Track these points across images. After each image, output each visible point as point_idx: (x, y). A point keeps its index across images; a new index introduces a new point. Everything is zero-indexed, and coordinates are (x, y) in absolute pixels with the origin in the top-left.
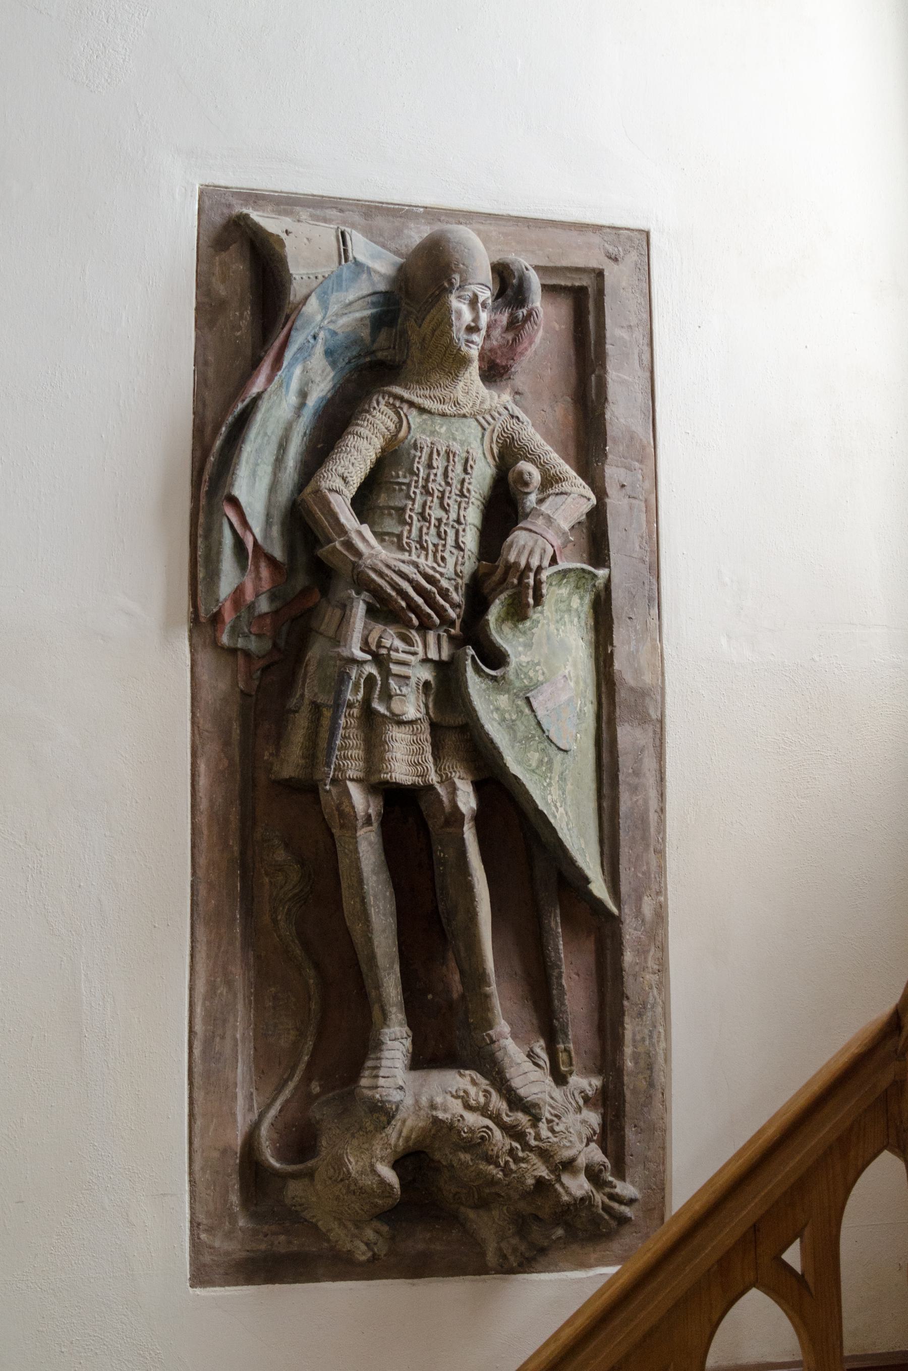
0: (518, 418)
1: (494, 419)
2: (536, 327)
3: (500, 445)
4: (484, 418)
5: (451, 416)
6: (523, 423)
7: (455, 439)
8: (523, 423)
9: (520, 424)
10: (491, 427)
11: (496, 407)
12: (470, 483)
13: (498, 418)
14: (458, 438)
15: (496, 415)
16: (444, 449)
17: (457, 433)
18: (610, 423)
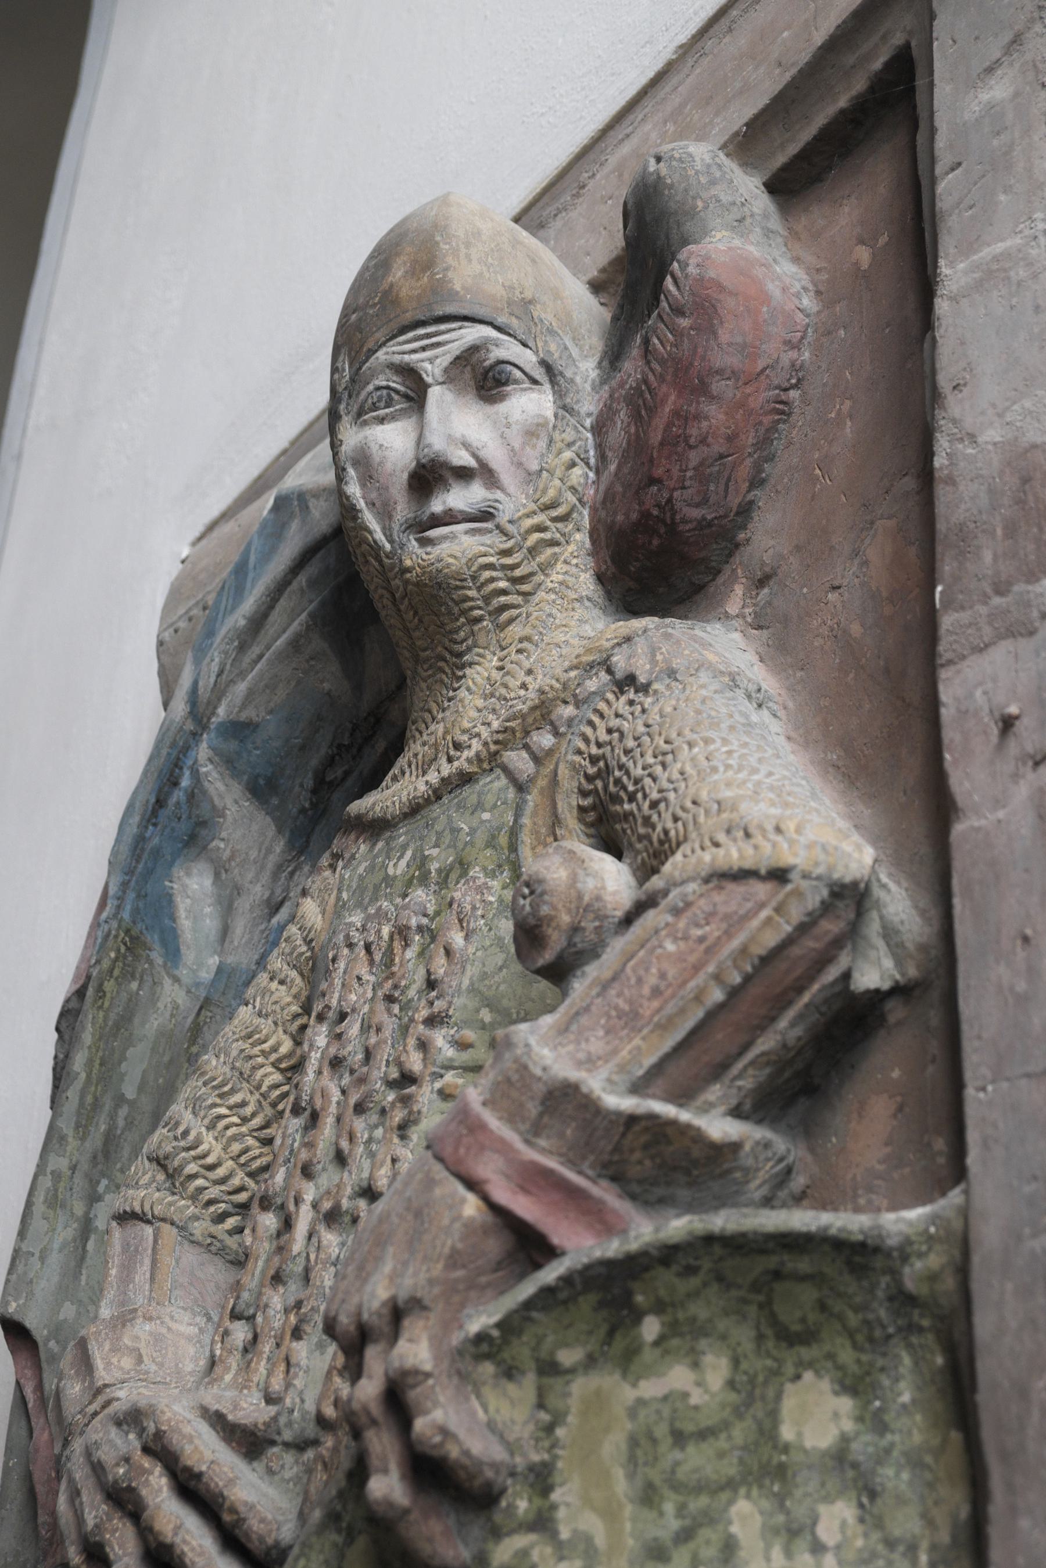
0: (630, 679)
1: (556, 733)
2: (684, 323)
3: (591, 816)
4: (526, 747)
5: (428, 802)
6: (645, 689)
7: (424, 880)
9: (640, 697)
11: (565, 686)
12: (431, 1021)
13: (570, 723)
14: (434, 866)
16: (386, 931)
17: (435, 852)
18: (951, 481)
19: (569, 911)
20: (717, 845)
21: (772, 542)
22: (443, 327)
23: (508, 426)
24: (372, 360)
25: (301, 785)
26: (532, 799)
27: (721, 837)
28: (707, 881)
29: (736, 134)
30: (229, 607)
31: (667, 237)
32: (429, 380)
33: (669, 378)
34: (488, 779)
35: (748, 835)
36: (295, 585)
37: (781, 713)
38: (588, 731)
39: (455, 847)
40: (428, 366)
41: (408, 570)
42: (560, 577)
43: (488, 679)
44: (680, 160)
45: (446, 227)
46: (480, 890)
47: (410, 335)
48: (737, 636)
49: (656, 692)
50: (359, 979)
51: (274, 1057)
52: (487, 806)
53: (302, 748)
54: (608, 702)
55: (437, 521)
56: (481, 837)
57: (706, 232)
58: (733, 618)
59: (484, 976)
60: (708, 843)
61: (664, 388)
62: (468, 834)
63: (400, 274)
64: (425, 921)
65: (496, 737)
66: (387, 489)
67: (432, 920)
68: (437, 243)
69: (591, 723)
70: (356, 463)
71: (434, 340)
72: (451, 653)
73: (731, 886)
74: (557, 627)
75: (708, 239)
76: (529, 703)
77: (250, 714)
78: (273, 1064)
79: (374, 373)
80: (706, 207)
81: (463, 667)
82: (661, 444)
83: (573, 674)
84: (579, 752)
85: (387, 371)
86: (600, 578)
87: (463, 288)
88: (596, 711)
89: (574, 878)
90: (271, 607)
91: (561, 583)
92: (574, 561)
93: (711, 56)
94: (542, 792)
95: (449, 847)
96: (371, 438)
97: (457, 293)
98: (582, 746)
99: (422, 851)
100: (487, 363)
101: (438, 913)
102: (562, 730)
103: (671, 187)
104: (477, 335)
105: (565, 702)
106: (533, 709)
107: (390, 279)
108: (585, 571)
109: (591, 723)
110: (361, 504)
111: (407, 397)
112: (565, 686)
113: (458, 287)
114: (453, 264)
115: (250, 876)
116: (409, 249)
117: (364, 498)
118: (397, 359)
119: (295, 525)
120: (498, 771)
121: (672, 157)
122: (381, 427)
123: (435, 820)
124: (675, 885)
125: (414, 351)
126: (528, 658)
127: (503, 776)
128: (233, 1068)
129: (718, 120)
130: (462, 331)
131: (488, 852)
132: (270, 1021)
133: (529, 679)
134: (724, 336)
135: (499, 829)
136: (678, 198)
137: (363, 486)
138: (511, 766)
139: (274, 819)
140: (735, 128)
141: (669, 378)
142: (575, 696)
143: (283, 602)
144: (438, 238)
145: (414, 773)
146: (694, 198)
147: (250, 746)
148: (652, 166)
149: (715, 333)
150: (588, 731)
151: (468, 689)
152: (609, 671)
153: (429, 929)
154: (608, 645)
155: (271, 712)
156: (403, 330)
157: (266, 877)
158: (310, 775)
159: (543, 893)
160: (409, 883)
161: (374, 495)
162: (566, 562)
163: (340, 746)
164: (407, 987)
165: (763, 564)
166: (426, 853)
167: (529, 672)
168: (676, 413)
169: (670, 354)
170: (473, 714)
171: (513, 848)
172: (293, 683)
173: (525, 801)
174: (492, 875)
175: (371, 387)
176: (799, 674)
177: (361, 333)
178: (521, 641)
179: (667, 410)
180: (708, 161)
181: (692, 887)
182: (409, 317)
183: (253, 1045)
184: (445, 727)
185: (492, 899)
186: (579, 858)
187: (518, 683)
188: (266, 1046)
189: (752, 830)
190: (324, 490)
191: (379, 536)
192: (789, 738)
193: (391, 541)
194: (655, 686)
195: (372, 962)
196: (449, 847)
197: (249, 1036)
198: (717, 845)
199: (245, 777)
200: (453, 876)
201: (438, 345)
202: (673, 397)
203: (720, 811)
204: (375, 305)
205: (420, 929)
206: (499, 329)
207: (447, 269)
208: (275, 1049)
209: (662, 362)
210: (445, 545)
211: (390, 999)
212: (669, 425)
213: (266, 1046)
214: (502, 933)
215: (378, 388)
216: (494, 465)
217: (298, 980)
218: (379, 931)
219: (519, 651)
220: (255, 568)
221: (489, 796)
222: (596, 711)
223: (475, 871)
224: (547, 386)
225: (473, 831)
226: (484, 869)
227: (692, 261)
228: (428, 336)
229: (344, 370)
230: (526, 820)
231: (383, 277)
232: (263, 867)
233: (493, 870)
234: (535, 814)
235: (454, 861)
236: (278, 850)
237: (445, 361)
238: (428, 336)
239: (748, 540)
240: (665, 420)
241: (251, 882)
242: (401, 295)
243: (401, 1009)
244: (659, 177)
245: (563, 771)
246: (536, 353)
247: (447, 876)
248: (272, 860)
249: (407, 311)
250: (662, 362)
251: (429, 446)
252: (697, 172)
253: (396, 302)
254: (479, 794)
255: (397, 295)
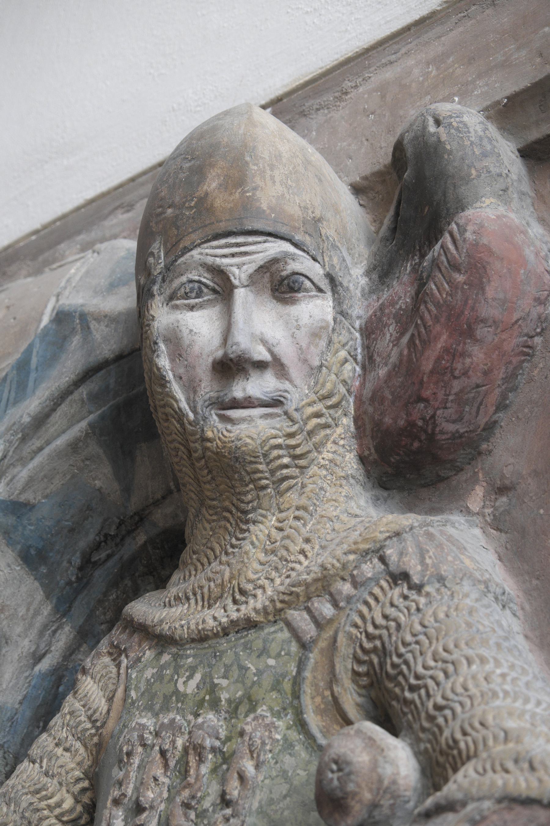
0: (405, 576)
1: (335, 604)
2: (460, 278)
3: (365, 681)
4: (308, 610)
5: (216, 635)
6: (419, 588)
7: (215, 704)
8: (419, 588)
9: (413, 595)
10: (328, 634)
11: (344, 566)
13: (349, 599)
14: (224, 696)
15: (346, 588)
16: (180, 742)
17: (224, 682)
19: (371, 790)
20: (507, 771)
21: (512, 460)
22: (251, 239)
23: (298, 328)
24: (187, 256)
25: (70, 562)
26: (313, 657)
27: (510, 765)
28: (500, 801)
29: (498, 103)
30: (12, 400)
31: (444, 194)
32: (236, 282)
33: (443, 320)
34: (272, 629)
35: (532, 768)
36: (76, 395)
37: (520, 613)
38: (365, 610)
39: (243, 683)
40: (235, 270)
41: (209, 440)
42: (330, 456)
43: (269, 536)
44: (458, 129)
45: (254, 148)
46: (270, 727)
47: (223, 241)
48: (477, 531)
49: (428, 594)
50: (156, 779)
51: (57, 811)
52: (273, 653)
53: (72, 530)
54: (382, 588)
55: (236, 404)
56: (267, 681)
57: (477, 198)
58: (474, 514)
59: (271, 802)
60: (498, 768)
61: (438, 328)
62: (255, 674)
63: (214, 185)
64: (217, 743)
65: (282, 597)
66: (194, 367)
67: (224, 743)
68: (247, 163)
69: (366, 603)
70: (167, 340)
71: (243, 249)
72: (238, 509)
73: (519, 809)
74: (328, 501)
75: (478, 204)
76: (312, 575)
77: (28, 496)
78: (57, 817)
79: (187, 268)
80: (479, 176)
81: (247, 522)
82: (432, 372)
83: (352, 557)
84: (356, 626)
85: (200, 268)
86: (362, 459)
87: (270, 208)
88: (371, 594)
89: (375, 765)
90: (53, 410)
91: (331, 461)
92: (342, 442)
93: (473, 21)
94: (322, 651)
95: (237, 681)
96: (182, 323)
97: (264, 211)
98: (359, 621)
99: (212, 678)
100: (284, 273)
101: (229, 739)
102: (342, 604)
103: (450, 153)
104: (278, 250)
105: (343, 579)
106: (316, 580)
107: (205, 187)
108: (350, 451)
109: (366, 603)
110: (170, 376)
111: (214, 291)
112: (344, 566)
113: (264, 206)
114: (261, 184)
115: (18, 629)
116: (221, 163)
117: (172, 370)
118: (210, 260)
119: (76, 340)
120: (282, 624)
121: (450, 124)
122: (190, 314)
123: (223, 652)
124: (473, 799)
125: (225, 256)
126: (304, 525)
127: (285, 629)
128: (23, 817)
129: (480, 83)
130: (267, 245)
131: (274, 695)
132: (55, 781)
133: (307, 547)
134: (490, 292)
135: (284, 676)
136: (456, 164)
137: (172, 361)
138: (295, 624)
139: (42, 585)
140: (497, 98)
141: (443, 320)
142: (352, 576)
143: (64, 407)
144: (248, 159)
145: (200, 603)
146: (469, 167)
147: (25, 522)
148: (432, 128)
149: (483, 289)
150: (365, 610)
151: (252, 543)
152: (383, 559)
153: (221, 751)
154: (381, 537)
155: (46, 497)
156: (217, 237)
157: (33, 633)
158: (78, 554)
159: (350, 774)
160: (201, 704)
161: (181, 371)
162: (335, 442)
163: (106, 536)
164: (202, 798)
165: (503, 477)
166: (216, 681)
167: (307, 541)
168: (446, 350)
169: (445, 301)
170: (256, 566)
171: (296, 695)
172: (68, 477)
173: (307, 658)
174: (278, 715)
175: (184, 279)
176: (535, 582)
177: (178, 229)
178: (298, 508)
179: (439, 346)
180: (481, 133)
181: (487, 804)
182: (223, 226)
183: (41, 800)
184: (231, 573)
185: (278, 737)
186: (379, 747)
187: (298, 548)
188: (52, 801)
189: (536, 765)
190: (105, 316)
191: (184, 405)
192: (526, 637)
193: (195, 412)
194: (428, 588)
195: (166, 766)
196: (237, 681)
197: (38, 792)
198: (507, 771)
199: (19, 547)
200: (242, 709)
201: (246, 254)
202: (444, 337)
203: (506, 740)
204: (191, 208)
205: (213, 750)
206: (296, 245)
207: (255, 189)
208: (59, 805)
209: (438, 305)
210: (243, 426)
211: (187, 806)
212: (439, 359)
213: (52, 801)
214: (286, 767)
215: (191, 281)
216: (285, 360)
217: (82, 750)
218: (174, 742)
219: (297, 518)
220: (37, 369)
221: (274, 645)
222: (371, 594)
223: (262, 710)
224: (329, 294)
225: (259, 673)
226: (271, 709)
227: (470, 228)
228: (238, 245)
229: (159, 258)
230: (307, 674)
231: (199, 183)
232: (31, 625)
233: (279, 712)
234: (314, 670)
235: (243, 695)
236: (46, 613)
237: (250, 268)
238: (238, 245)
239: (490, 452)
240: (436, 353)
241: (19, 636)
242: (216, 205)
243: (197, 816)
244: (439, 141)
245: (341, 639)
246: (323, 266)
247: (237, 708)
248: (40, 621)
249: (221, 221)
250: (438, 305)
251: (237, 344)
252: (472, 143)
253: (210, 210)
254: (265, 641)
255: (212, 205)
